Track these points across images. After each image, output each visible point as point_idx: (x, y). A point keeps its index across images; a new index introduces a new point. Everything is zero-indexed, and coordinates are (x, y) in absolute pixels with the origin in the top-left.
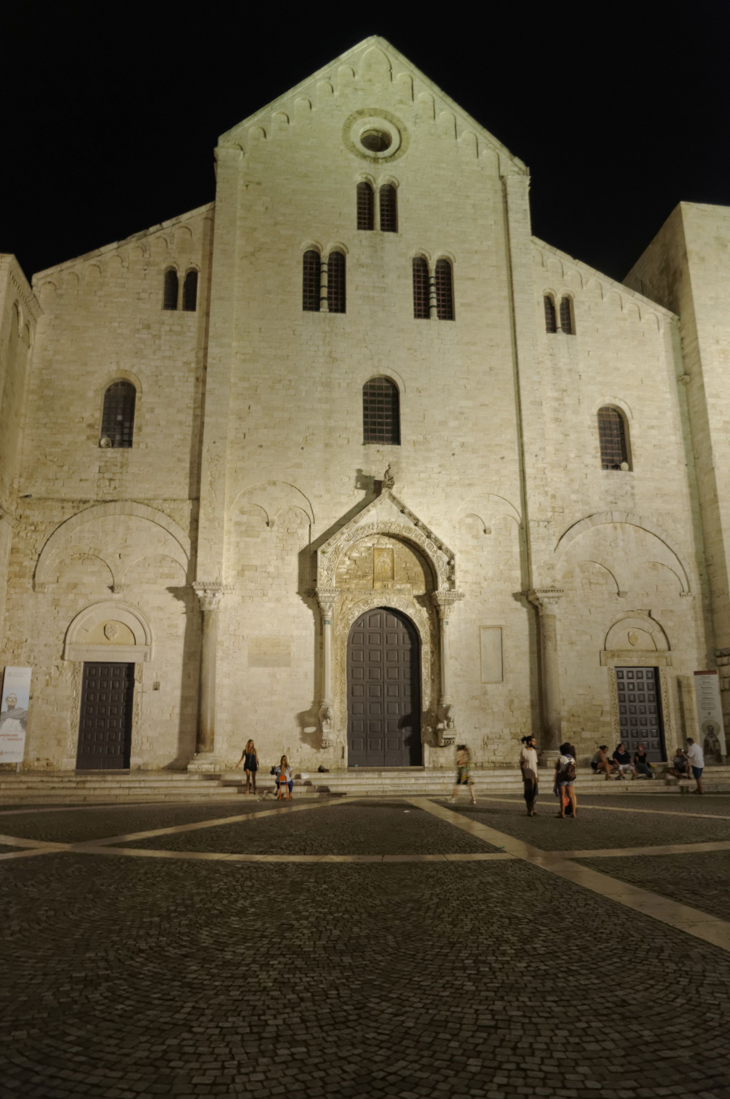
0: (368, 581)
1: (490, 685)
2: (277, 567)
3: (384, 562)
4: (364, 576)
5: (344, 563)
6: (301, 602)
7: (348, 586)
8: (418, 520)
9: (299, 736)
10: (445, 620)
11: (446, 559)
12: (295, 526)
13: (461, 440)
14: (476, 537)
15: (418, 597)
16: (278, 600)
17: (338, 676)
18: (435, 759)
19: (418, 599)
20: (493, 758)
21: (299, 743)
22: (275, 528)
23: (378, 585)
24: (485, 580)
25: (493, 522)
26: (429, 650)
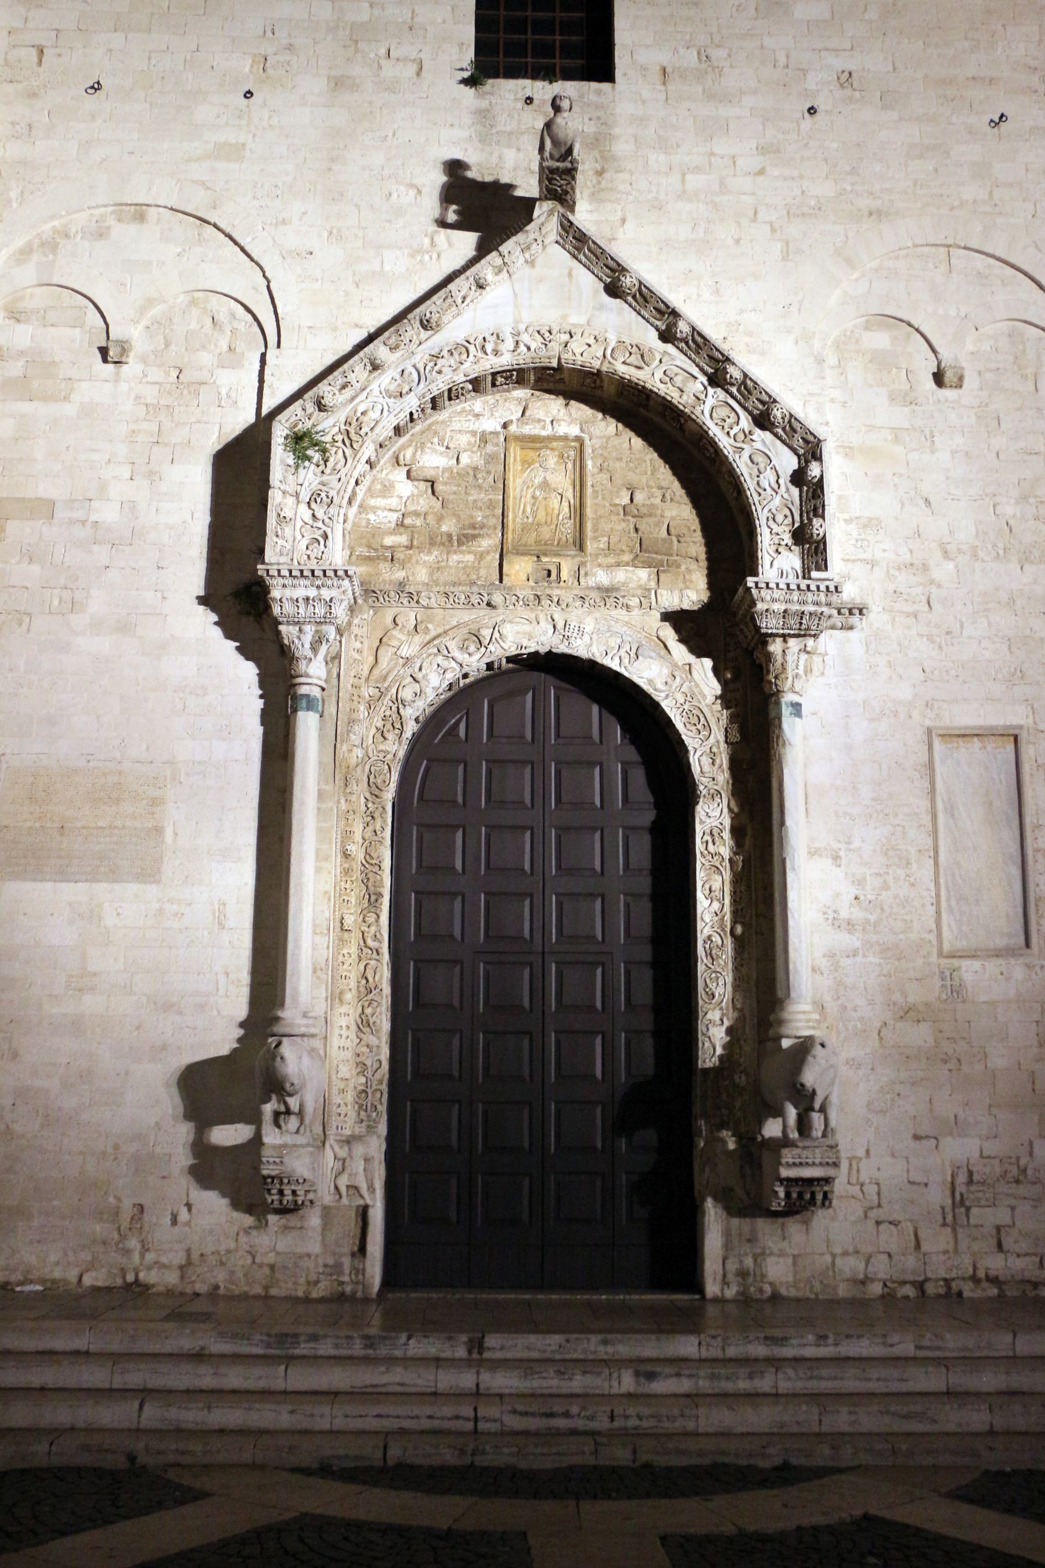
0: (481, 556)
1: (976, 964)
2: (130, 507)
3: (545, 485)
4: (466, 538)
5: (387, 489)
6: (217, 632)
7: (400, 575)
8: (675, 314)
9: (183, 1159)
10: (788, 698)
11: (788, 462)
12: (206, 358)
13: (839, 63)
14: (907, 399)
15: (676, 619)
16: (125, 628)
17: (349, 921)
18: (749, 1262)
19: (677, 629)
20: (995, 1264)
21: (183, 1186)
22: (132, 367)
23: (519, 569)
24: (946, 554)
25: (970, 347)
26: (727, 822)
